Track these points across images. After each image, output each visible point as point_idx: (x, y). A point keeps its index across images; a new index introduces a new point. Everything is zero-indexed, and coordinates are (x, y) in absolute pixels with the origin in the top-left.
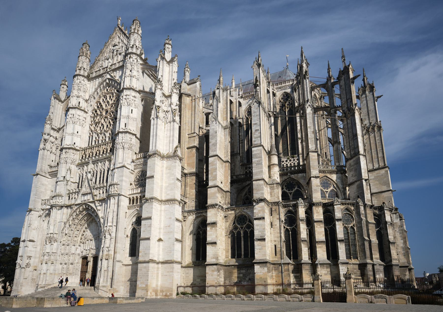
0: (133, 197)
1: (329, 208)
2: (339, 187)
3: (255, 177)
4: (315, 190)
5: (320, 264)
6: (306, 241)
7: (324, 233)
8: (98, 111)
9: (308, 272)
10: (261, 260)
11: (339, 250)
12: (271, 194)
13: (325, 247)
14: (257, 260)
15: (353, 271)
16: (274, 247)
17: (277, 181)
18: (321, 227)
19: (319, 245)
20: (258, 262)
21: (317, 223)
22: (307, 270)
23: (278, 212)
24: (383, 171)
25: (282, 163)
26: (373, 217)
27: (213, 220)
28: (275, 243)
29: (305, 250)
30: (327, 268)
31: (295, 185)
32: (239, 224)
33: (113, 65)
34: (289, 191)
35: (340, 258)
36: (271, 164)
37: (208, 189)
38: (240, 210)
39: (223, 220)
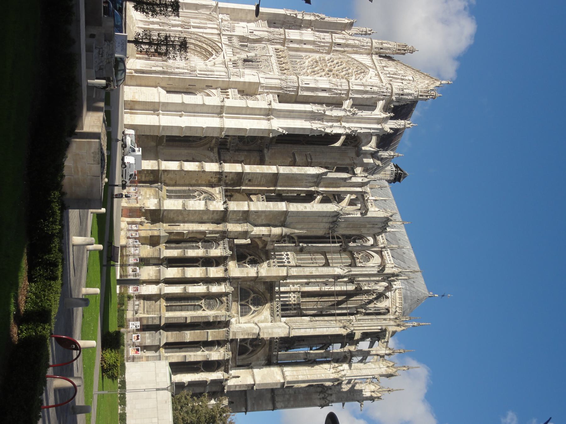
0: (228, 92)
2: (255, 318)
4: (243, 271)
7: (194, 276)
8: (332, 64)
9: (151, 254)
10: (163, 204)
13: (178, 277)
14: (163, 202)
18: (201, 274)
19: (180, 270)
20: (161, 202)
21: (205, 270)
22: (154, 254)
26: (216, 339)
27: (206, 167)
29: (174, 253)
30: (156, 276)
35: (166, 288)
39: (207, 182)
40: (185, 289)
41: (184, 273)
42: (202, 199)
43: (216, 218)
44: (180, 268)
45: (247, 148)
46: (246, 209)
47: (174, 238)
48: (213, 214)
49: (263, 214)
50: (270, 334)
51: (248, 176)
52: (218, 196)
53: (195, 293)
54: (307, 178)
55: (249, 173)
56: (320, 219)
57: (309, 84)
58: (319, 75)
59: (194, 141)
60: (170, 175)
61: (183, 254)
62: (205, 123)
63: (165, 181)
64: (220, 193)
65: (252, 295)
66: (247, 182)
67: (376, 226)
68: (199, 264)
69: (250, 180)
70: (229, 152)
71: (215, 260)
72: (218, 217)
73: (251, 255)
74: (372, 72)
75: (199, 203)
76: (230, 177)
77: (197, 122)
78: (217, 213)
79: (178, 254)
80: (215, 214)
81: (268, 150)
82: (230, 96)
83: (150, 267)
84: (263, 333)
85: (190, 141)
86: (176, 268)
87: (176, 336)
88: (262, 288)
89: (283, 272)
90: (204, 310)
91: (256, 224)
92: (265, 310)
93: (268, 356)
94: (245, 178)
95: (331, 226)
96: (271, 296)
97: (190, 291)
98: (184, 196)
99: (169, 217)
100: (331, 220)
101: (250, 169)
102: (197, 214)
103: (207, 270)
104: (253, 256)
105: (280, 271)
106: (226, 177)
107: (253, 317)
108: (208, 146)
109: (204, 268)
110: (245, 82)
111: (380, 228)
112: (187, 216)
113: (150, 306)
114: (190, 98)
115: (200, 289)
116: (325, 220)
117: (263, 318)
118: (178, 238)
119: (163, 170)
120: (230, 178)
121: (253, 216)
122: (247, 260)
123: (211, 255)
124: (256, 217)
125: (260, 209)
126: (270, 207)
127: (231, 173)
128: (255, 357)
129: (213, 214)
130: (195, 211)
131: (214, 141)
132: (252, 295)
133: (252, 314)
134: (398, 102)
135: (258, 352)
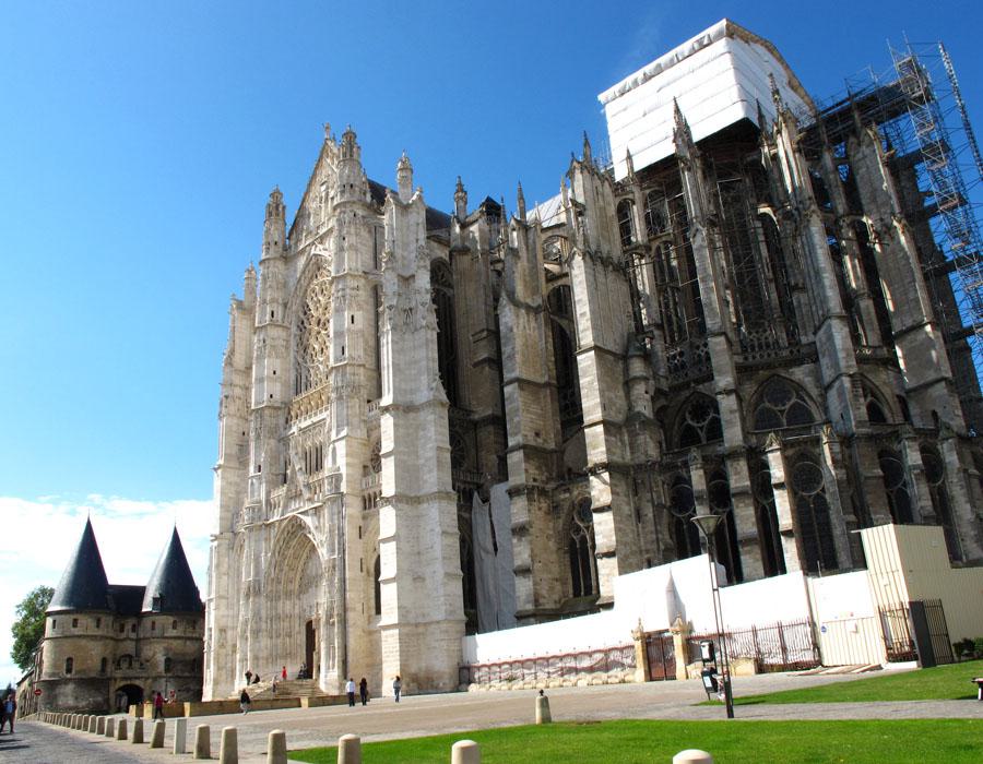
0: (369, 495)
3: (587, 419)
7: (754, 519)
8: (305, 321)
11: (785, 555)
12: (631, 448)
18: (746, 506)
19: (746, 549)
28: (646, 556)
32: (582, 520)
39: (550, 517)
40: (788, 534)
41: (749, 541)
42: (586, 524)
43: (625, 488)
44: (741, 550)
45: (473, 451)
46: (600, 428)
48: (618, 494)
49: (607, 393)
50: (848, 355)
53: (792, 511)
54: (521, 327)
56: (601, 287)
58: (326, 339)
60: (544, 592)
63: (555, 602)
65: (767, 405)
66: (540, 440)
67: (600, 189)
69: (537, 434)
70: (482, 485)
71: (711, 481)
72: (623, 483)
73: (685, 420)
74: (318, 250)
75: (600, 524)
78: (616, 486)
81: (473, 412)
84: (849, 367)
86: (742, 558)
88: (749, 389)
89: (717, 344)
90: (823, 490)
91: (626, 408)
92: (792, 378)
93: (877, 364)
94: (532, 443)
95: (611, 268)
96: (762, 368)
97: (791, 521)
98: (583, 560)
100: (600, 268)
101: (516, 434)
103: (735, 495)
104: (684, 415)
105: (718, 348)
106: (535, 480)
109: (733, 500)
110: (348, 464)
111: (603, 183)
115: (783, 503)
116: (601, 279)
117: (810, 379)
119: (536, 606)
120: (537, 472)
121: (613, 414)
122: (695, 425)
124: (614, 408)
125: (599, 400)
126: (591, 383)
127: (526, 471)
128: (886, 391)
130: (618, 530)
132: (767, 405)
133: (804, 401)
134: (365, 194)
135: (873, 383)
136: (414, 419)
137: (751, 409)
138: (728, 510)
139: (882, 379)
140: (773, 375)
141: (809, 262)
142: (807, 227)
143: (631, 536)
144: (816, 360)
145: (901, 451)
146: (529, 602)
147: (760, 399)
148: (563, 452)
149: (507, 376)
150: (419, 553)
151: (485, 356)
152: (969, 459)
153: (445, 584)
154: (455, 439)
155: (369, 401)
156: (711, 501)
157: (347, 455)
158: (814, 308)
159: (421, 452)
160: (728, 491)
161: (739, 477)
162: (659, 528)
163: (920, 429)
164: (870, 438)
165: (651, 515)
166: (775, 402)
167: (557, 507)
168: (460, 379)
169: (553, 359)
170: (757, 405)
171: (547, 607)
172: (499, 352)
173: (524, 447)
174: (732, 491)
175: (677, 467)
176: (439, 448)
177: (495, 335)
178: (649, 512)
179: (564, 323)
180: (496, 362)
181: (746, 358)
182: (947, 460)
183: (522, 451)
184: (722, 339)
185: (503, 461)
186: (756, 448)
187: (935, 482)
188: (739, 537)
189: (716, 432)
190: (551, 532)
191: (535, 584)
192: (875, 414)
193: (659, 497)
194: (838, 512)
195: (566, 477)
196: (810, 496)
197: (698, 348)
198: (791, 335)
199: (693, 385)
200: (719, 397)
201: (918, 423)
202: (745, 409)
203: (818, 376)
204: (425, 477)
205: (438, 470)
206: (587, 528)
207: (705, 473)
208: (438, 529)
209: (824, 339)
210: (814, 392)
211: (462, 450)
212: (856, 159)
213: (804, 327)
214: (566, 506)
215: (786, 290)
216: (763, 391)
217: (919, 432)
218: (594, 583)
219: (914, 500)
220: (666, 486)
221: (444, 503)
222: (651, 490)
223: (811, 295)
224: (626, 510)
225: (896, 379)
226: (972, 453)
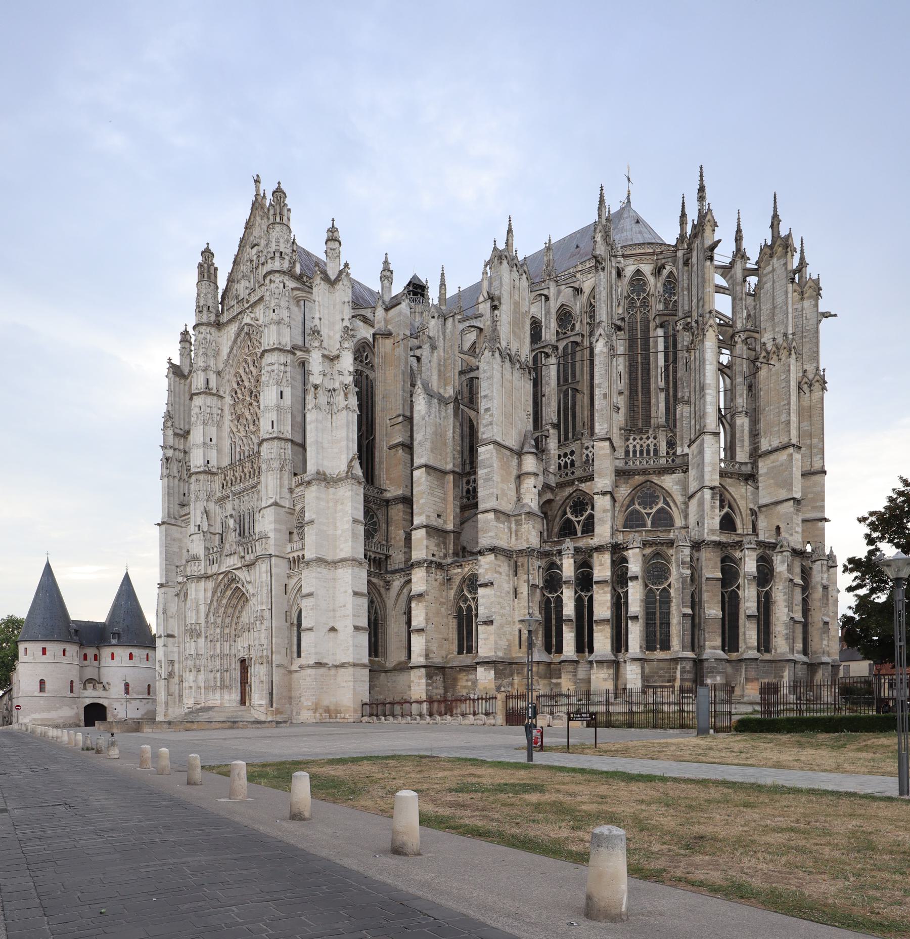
0: (294, 557)
1: (625, 553)
5: (597, 662)
6: (571, 620)
7: (609, 604)
9: (570, 677)
10: (486, 657)
13: (609, 630)
15: (658, 673)
16: (517, 633)
17: (530, 507)
19: (599, 627)
21: (598, 585)
23: (526, 569)
24: (783, 456)
25: (585, 451)
30: (608, 667)
31: (587, 504)
32: (470, 592)
33: (252, 294)
34: (576, 517)
35: (630, 651)
36: (522, 472)
37: (413, 532)
38: (470, 566)
39: (445, 587)
41: (603, 621)
42: (473, 596)
44: (595, 628)
47: (540, 639)
48: (500, 573)
51: (432, 518)
52: (467, 569)
55: (428, 516)
57: (273, 422)
59: (376, 612)
61: (570, 623)
62: (346, 592)
64: (461, 565)
65: (637, 507)
66: (440, 521)
68: (586, 596)
69: (439, 516)
72: (506, 564)
75: (483, 597)
76: (433, 548)
77: (344, 606)
78: (500, 566)
79: (571, 632)
80: (501, 570)
82: (300, 553)
83: (593, 677)
85: (376, 620)
86: (595, 635)
87: (712, 632)
88: (624, 491)
98: (467, 626)
99: (506, 647)
101: (420, 514)
102: (501, 600)
106: (433, 555)
107: (675, 504)
108: (382, 590)
109: (594, 586)
112: (504, 618)
113: (660, 677)
114: (306, 617)
118: (541, 632)
120: (436, 549)
123: (573, 574)
127: (427, 547)
129: (500, 573)
131: (375, 580)
132: (637, 507)
136: (334, 494)
137: (624, 509)
138: (589, 594)
139: (740, 493)
140: (646, 482)
141: (697, 376)
142: (702, 341)
143: (508, 608)
144: (686, 471)
145: (741, 559)
146: (420, 656)
147: (632, 502)
148: (460, 533)
149: (417, 461)
150: (334, 610)
151: (401, 440)
152: (798, 570)
153: (354, 637)
154: (368, 512)
155: (295, 474)
156: (577, 585)
157: (276, 522)
158: (693, 422)
159: (338, 524)
160: (592, 578)
161: (602, 568)
162: (530, 604)
163: (761, 542)
164: (718, 545)
165: (526, 593)
166: (645, 504)
167: (450, 579)
168: (376, 460)
169: (458, 448)
170: (629, 506)
171: (435, 660)
172: (412, 437)
173: (426, 526)
174: (595, 579)
175: (552, 554)
176: (355, 521)
177: (409, 420)
178: (524, 590)
179: (472, 414)
180: (408, 447)
181: (626, 463)
182: (778, 571)
183: (424, 529)
184: (607, 443)
185: (408, 539)
186: (621, 544)
187: (764, 587)
188: (595, 618)
189: (589, 527)
190: (444, 601)
191: (427, 641)
192: (727, 523)
193: (533, 579)
194: (678, 606)
195: (461, 554)
196: (658, 590)
197: (587, 448)
198: (671, 445)
199: (576, 483)
200: (596, 497)
201: (762, 537)
202: (617, 509)
203: (685, 487)
204: (341, 546)
205: (353, 541)
206: (474, 599)
207: (575, 562)
208: (350, 592)
209: (695, 453)
210: (679, 499)
211: (375, 524)
212: (765, 272)
213: (682, 438)
214: (457, 580)
215: (672, 402)
216: (636, 494)
217: (760, 544)
218: (474, 645)
219: (742, 601)
220: (541, 570)
221: (357, 569)
222: (528, 573)
223: (693, 409)
224: (507, 587)
225: (753, 494)
226: (802, 564)
